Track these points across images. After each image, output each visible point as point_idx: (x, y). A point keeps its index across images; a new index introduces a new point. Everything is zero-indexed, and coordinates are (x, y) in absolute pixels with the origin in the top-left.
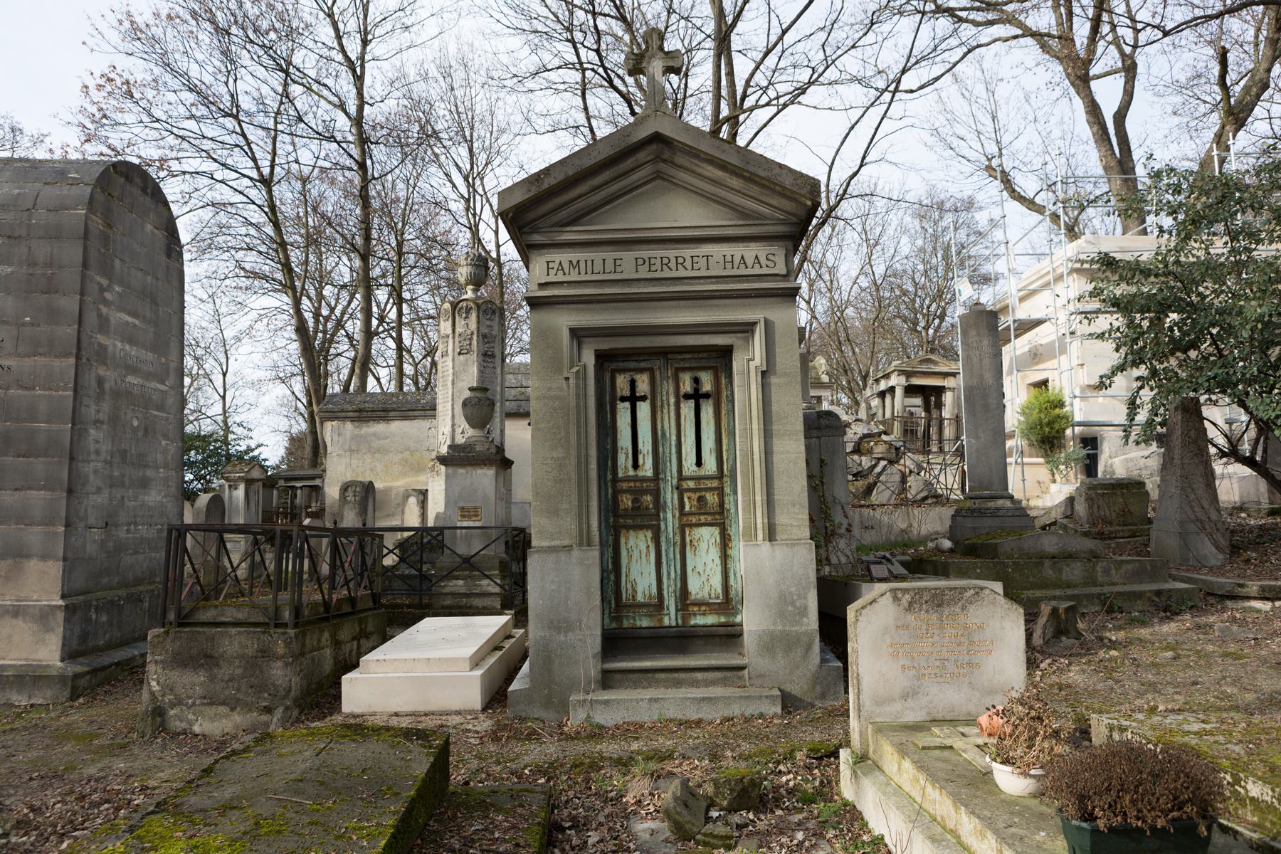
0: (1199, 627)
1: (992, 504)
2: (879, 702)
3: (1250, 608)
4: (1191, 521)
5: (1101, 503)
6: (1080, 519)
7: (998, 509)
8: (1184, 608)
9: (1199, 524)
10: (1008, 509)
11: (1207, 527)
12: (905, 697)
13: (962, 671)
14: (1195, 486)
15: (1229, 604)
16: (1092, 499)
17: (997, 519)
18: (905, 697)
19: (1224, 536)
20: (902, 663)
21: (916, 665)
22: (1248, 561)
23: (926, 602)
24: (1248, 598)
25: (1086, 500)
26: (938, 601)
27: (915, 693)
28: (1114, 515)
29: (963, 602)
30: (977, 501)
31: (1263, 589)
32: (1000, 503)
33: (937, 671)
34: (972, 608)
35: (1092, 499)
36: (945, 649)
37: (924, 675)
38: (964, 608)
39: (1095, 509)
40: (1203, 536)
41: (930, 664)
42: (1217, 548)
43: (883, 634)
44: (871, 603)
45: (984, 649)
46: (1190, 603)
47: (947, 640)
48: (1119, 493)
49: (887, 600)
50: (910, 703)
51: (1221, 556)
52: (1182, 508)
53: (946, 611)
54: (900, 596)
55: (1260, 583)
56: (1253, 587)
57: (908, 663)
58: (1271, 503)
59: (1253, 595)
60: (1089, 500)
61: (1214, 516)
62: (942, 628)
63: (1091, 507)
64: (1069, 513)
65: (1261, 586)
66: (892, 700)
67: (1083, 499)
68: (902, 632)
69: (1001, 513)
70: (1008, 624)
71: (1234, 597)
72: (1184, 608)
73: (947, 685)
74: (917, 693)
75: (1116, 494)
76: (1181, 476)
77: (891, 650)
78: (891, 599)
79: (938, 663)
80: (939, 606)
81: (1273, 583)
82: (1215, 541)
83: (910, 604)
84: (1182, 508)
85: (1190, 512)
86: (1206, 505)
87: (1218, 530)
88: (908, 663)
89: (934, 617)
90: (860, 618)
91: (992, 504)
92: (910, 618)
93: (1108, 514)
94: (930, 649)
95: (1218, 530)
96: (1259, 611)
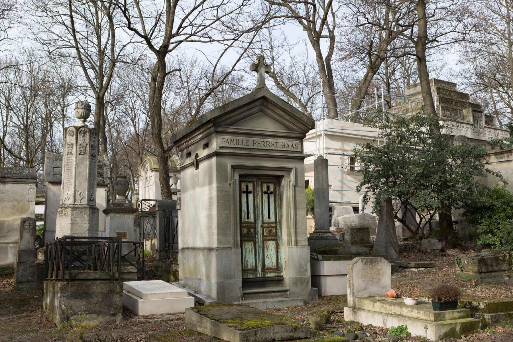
1: (325, 235)
6: (347, 241)
7: (327, 237)
10: (331, 237)
15: (405, 269)
17: (327, 241)
22: (405, 256)
26: (372, 262)
28: (359, 240)
31: (416, 264)
32: (328, 234)
34: (379, 264)
39: (353, 238)
40: (392, 247)
42: (396, 252)
46: (395, 270)
51: (397, 255)
55: (415, 262)
56: (413, 264)
60: (351, 234)
61: (395, 240)
63: (352, 237)
64: (342, 239)
65: (415, 263)
67: (349, 234)
69: (328, 239)
71: (407, 267)
80: (372, 263)
81: (423, 262)
83: (366, 262)
86: (393, 236)
89: (371, 266)
91: (325, 235)
92: (365, 267)
96: (414, 272)
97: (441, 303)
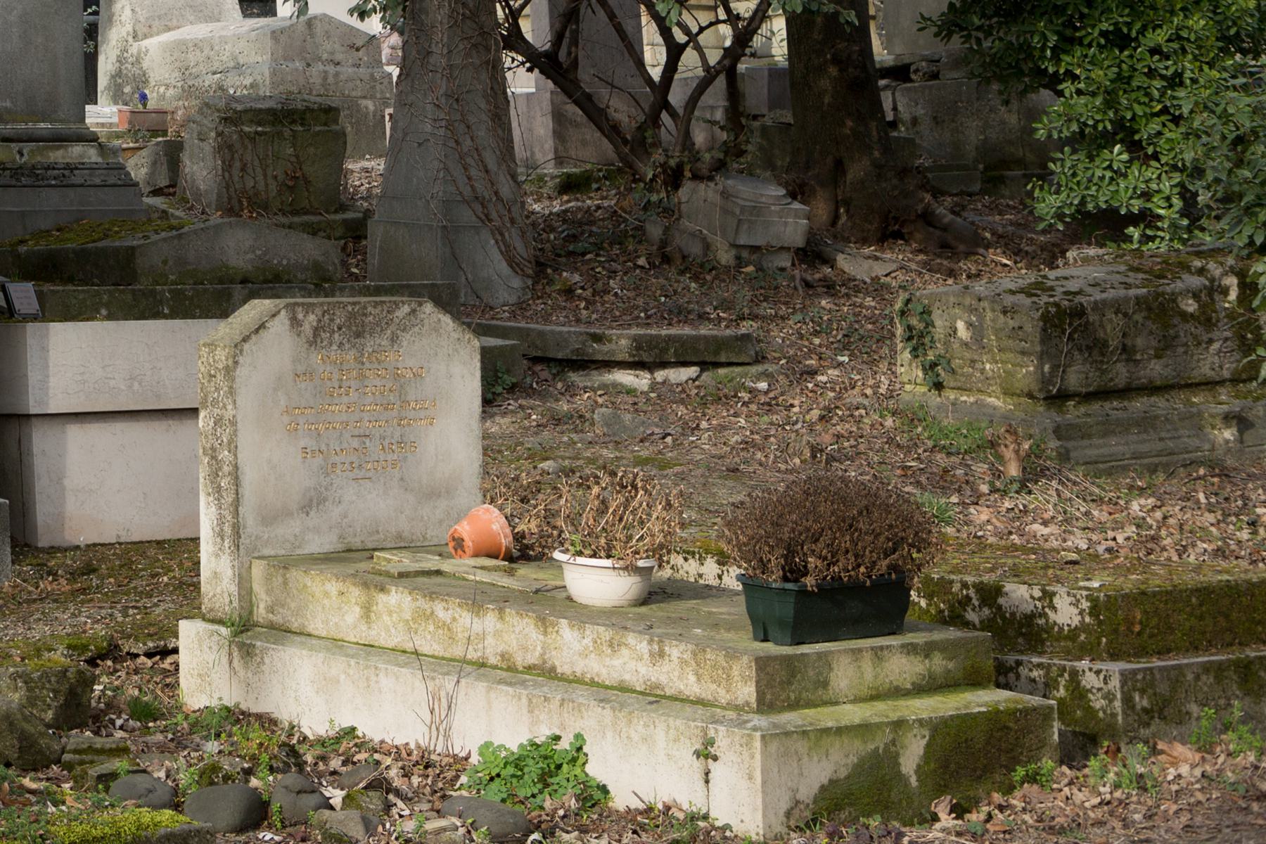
0: (557, 420)
1: (58, 156)
2: (269, 518)
3: (615, 385)
4: (465, 201)
5: (248, 157)
6: (198, 195)
7: (71, 168)
8: (499, 389)
9: (479, 208)
10: (93, 168)
11: (494, 215)
12: (307, 507)
13: (390, 457)
14: (472, 119)
15: (575, 377)
16: (230, 147)
17: (71, 193)
18: (306, 508)
19: (523, 233)
20: (302, 444)
21: (323, 448)
22: (569, 292)
23: (340, 329)
24: (609, 365)
25: (219, 149)
26: (357, 330)
27: (322, 501)
28: (273, 187)
29: (393, 327)
30: (27, 147)
31: (639, 344)
32: (76, 152)
33: (354, 459)
34: (406, 338)
35: (230, 147)
36: (366, 416)
37: (334, 465)
38: (394, 339)
39: (236, 173)
40: (485, 234)
41: (345, 445)
42: (511, 262)
43: (275, 390)
44: (257, 331)
45: (422, 414)
46: (510, 380)
47: (369, 398)
48: (287, 133)
49: (280, 325)
50: (314, 519)
51: (516, 282)
52: (446, 169)
53: (369, 344)
54: (300, 316)
55: (635, 331)
56: (621, 342)
57: (311, 443)
58: (559, 160)
59: (620, 357)
60: (226, 149)
61: (506, 189)
62: (362, 377)
63: (228, 167)
64: (163, 182)
65: (635, 338)
66: (287, 514)
67: (208, 147)
68: (303, 385)
69: (77, 178)
70: (457, 369)
71: (584, 364)
72: (499, 389)
73: (368, 484)
74: (325, 500)
75: (280, 134)
76: (447, 96)
77: (286, 419)
78: (287, 322)
79: (355, 443)
80: (358, 335)
81: (687, 331)
82: (507, 246)
83: (316, 331)
84: (446, 169)
85: (462, 180)
86: (492, 163)
87: (512, 221)
88: (311, 443)
89: (351, 355)
90: (241, 360)
91: (58, 156)
92: (316, 358)
93: (261, 186)
94: (344, 417)
95: (512, 221)
96: (630, 391)
97: (803, 593)
